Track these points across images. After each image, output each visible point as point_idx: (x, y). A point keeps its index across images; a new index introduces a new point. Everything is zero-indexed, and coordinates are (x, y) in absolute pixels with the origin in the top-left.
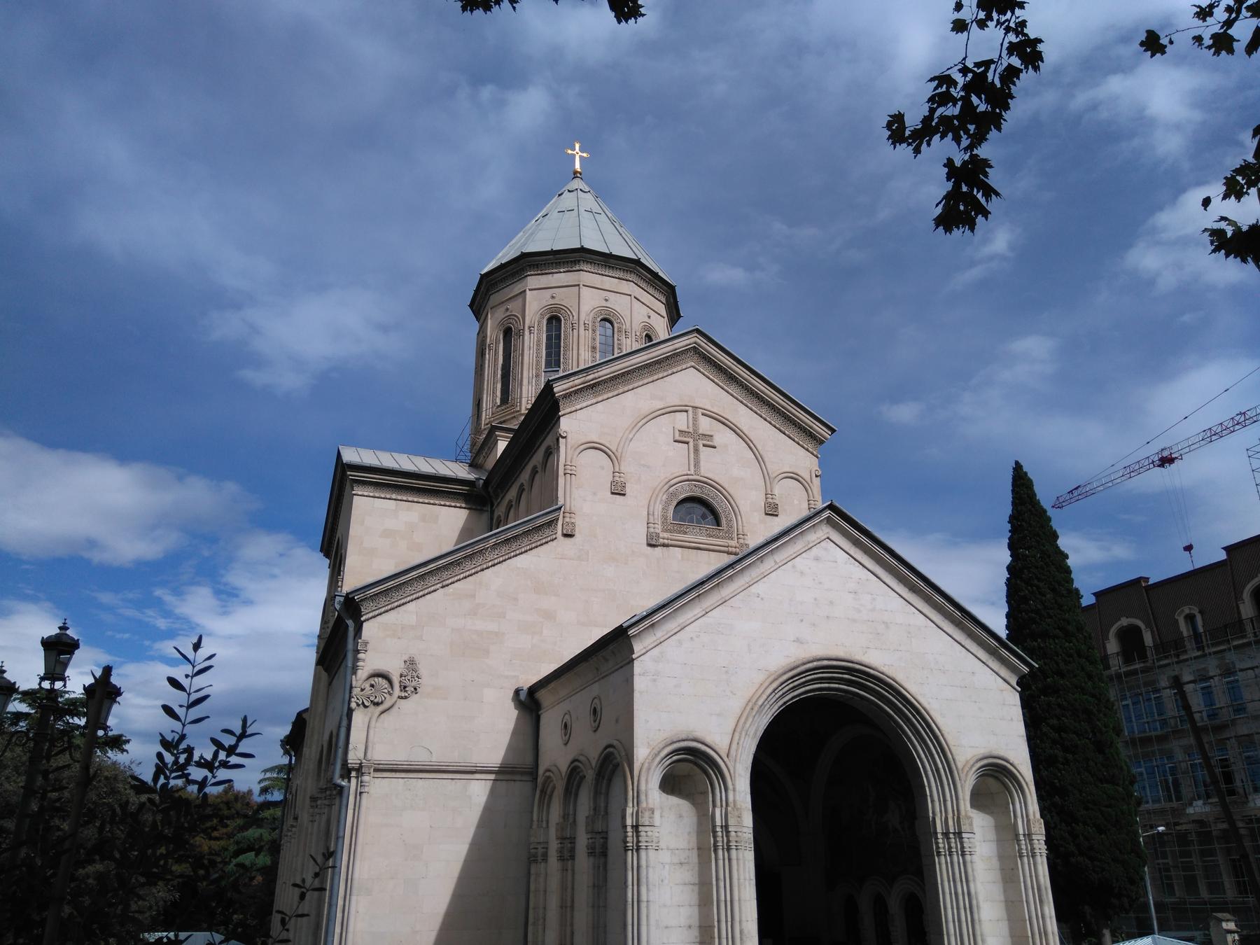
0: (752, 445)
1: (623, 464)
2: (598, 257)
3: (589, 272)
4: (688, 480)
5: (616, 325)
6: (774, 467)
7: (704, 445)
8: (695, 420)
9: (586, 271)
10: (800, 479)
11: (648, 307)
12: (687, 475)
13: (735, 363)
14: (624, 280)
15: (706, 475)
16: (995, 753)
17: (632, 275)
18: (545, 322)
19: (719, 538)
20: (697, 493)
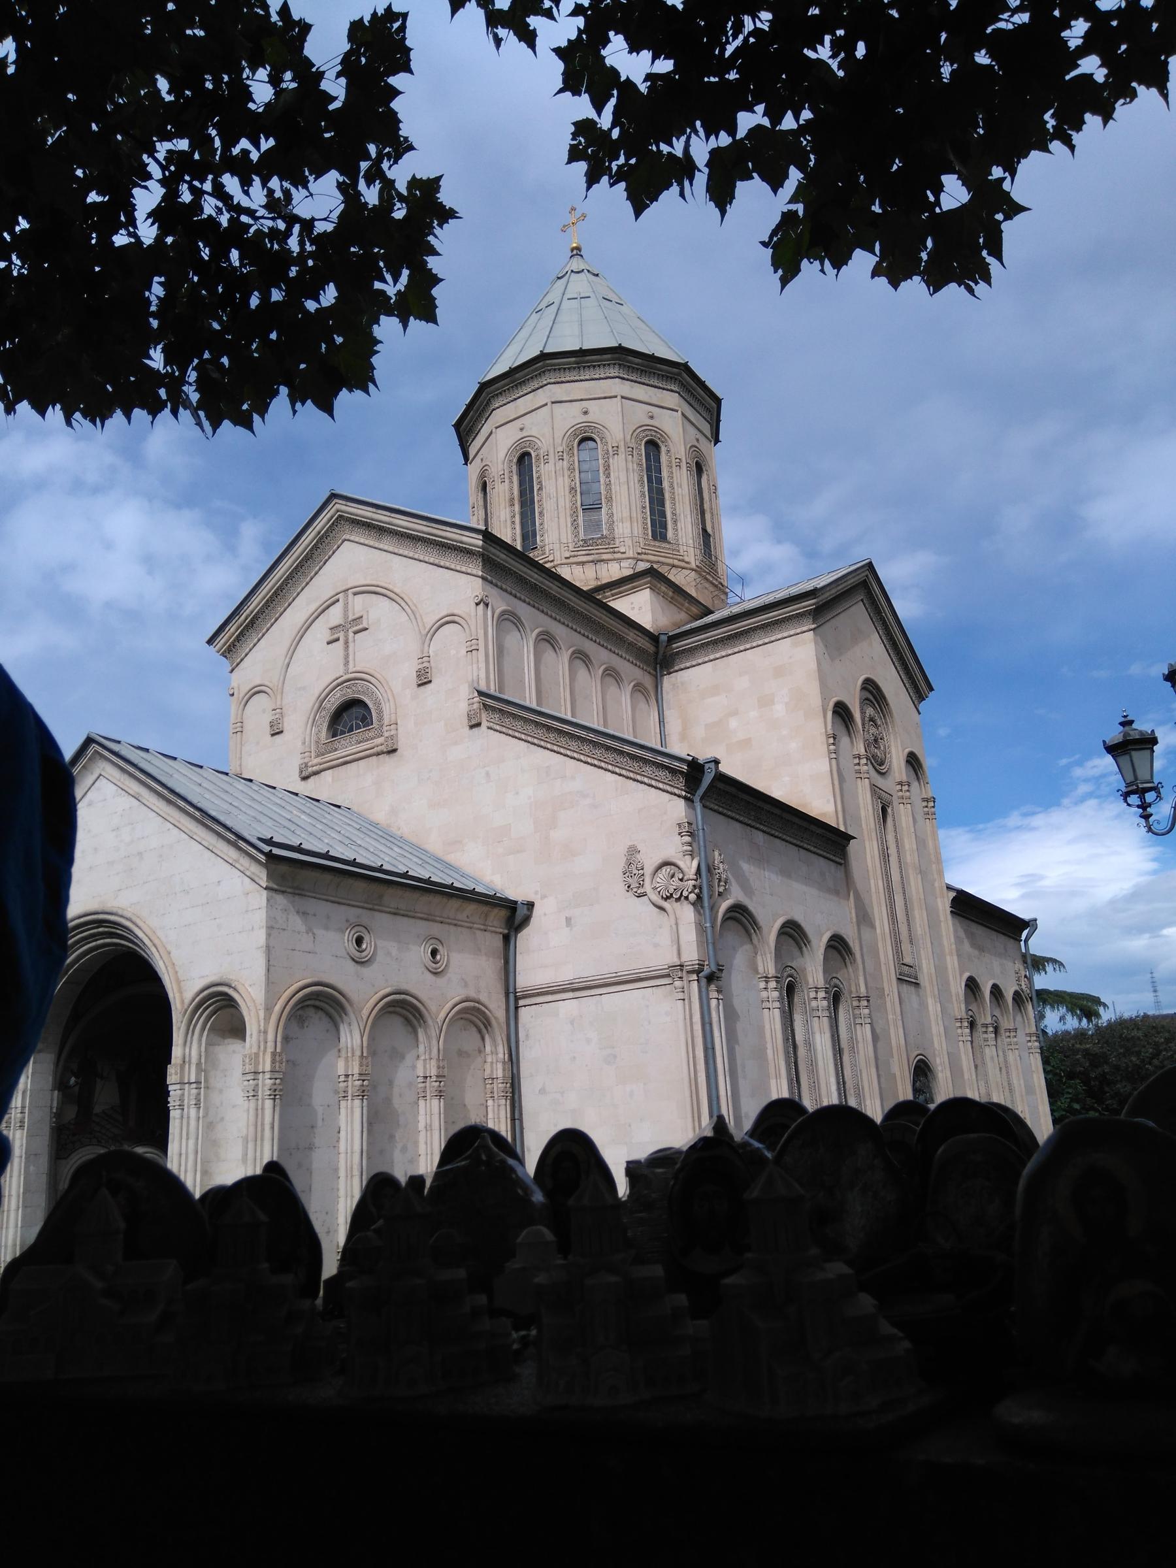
0: (403, 604)
1: (279, 697)
2: (503, 382)
3: (502, 406)
4: (338, 685)
5: (533, 456)
6: (430, 620)
7: (355, 633)
8: (346, 605)
9: (498, 408)
10: (456, 619)
11: (582, 400)
12: (337, 679)
13: (374, 510)
14: (538, 389)
15: (354, 670)
16: (225, 979)
17: (547, 374)
18: (481, 495)
19: (368, 740)
20: (351, 695)
